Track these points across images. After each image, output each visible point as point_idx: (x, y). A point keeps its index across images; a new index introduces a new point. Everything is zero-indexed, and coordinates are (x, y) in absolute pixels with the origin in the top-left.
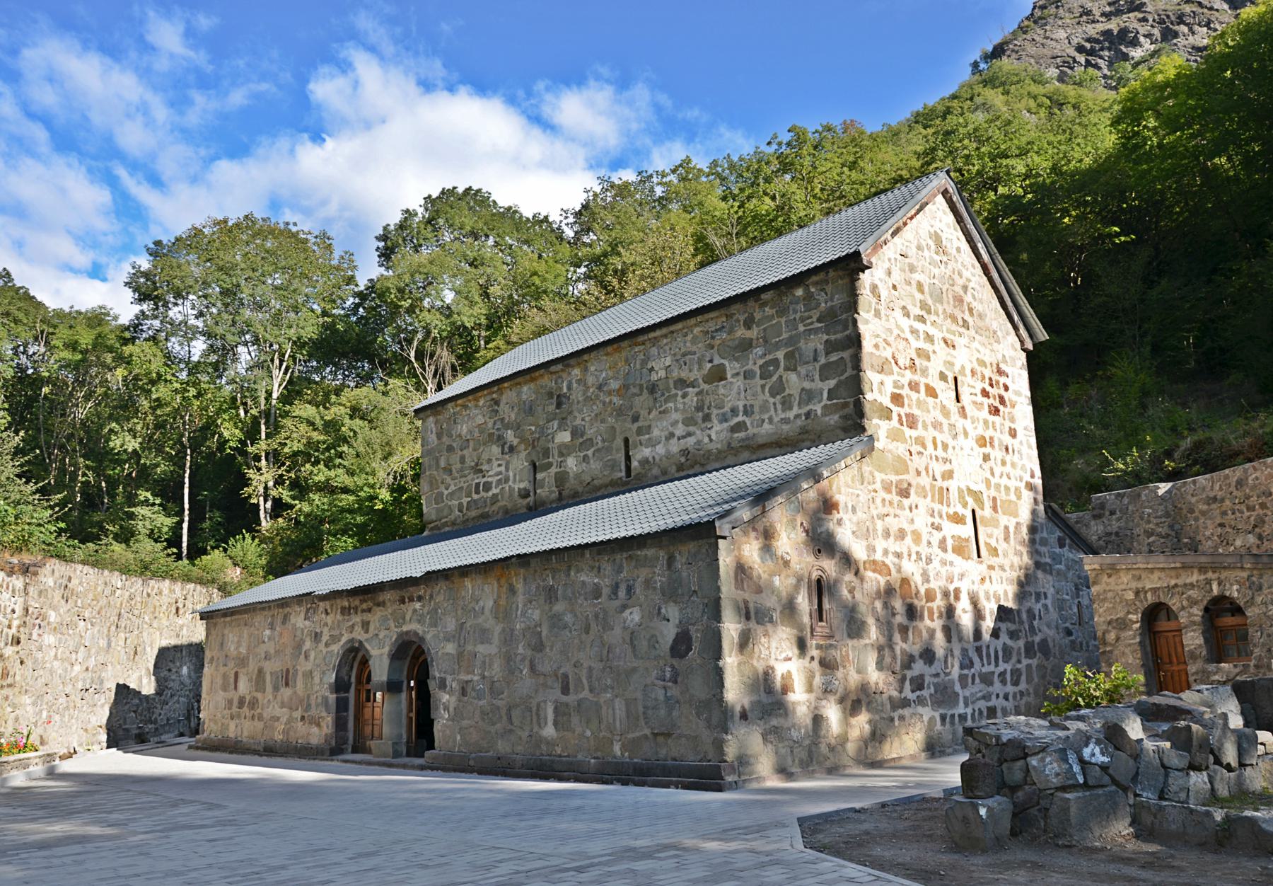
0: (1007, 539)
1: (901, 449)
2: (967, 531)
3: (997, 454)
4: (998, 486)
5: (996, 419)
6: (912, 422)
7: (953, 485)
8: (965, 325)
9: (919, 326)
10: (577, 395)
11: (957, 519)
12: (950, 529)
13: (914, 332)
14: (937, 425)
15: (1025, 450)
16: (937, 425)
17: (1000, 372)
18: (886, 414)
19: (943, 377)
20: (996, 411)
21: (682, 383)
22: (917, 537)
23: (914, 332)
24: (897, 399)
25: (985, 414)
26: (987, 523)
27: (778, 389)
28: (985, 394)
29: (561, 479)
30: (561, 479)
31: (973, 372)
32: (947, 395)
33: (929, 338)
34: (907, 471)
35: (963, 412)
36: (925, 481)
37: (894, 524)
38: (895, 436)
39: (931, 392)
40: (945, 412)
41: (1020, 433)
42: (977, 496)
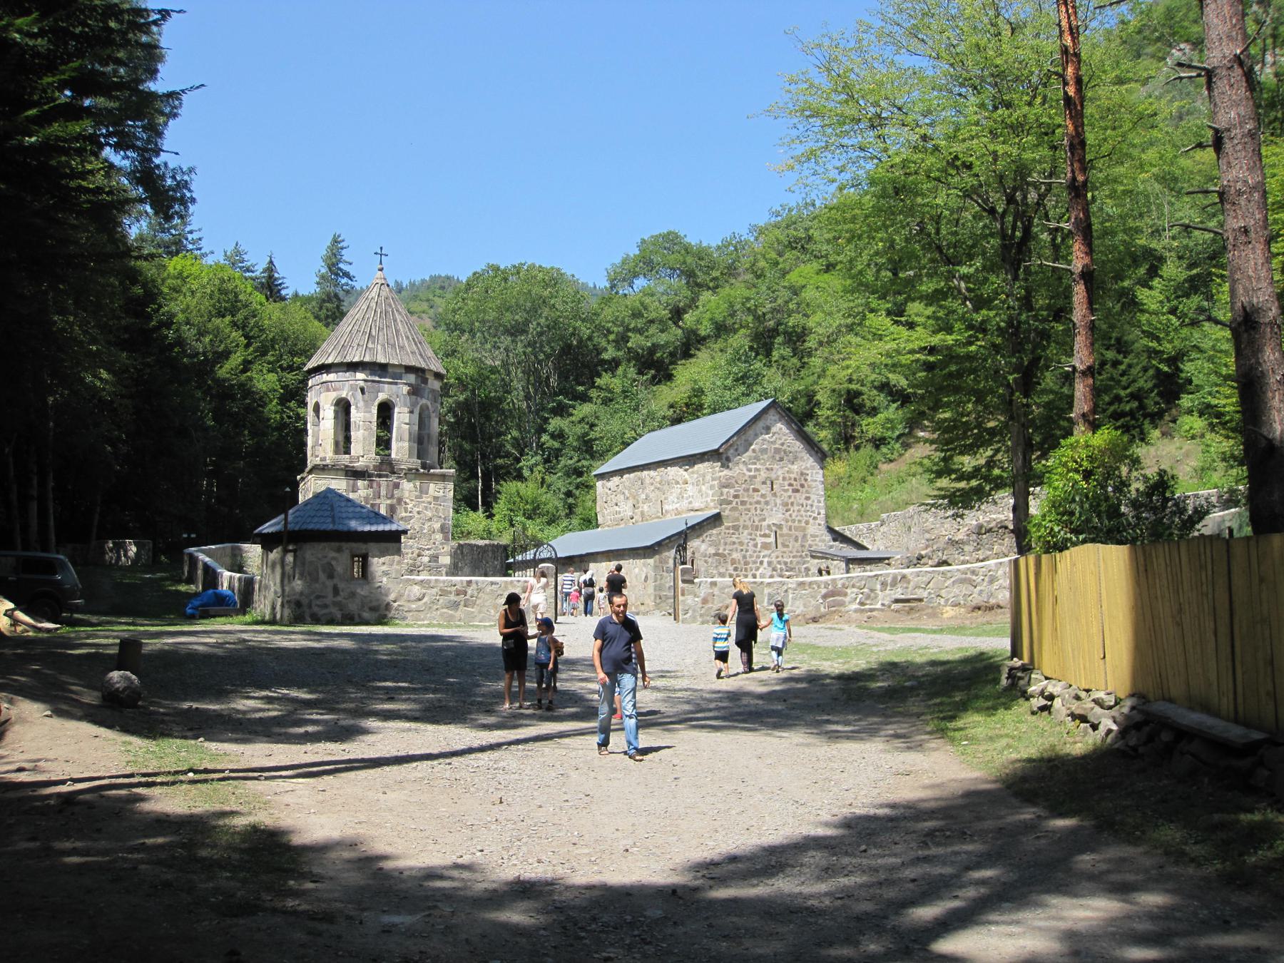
0: (796, 540)
1: (736, 514)
2: (772, 539)
3: (796, 508)
4: (794, 521)
5: (797, 495)
6: (743, 503)
7: (765, 524)
8: (781, 459)
9: (753, 467)
10: (648, 481)
11: (765, 536)
12: (760, 540)
13: (750, 470)
14: (758, 502)
15: (816, 504)
16: (758, 502)
17: (802, 474)
18: (730, 503)
19: (764, 483)
20: (797, 491)
21: (677, 483)
22: (741, 543)
23: (750, 470)
24: (736, 497)
25: (790, 493)
26: (782, 535)
27: (700, 491)
28: (790, 485)
29: (642, 513)
30: (642, 513)
31: (784, 479)
32: (765, 490)
33: (757, 470)
34: (737, 519)
35: (775, 495)
36: (749, 523)
37: (729, 540)
38: (733, 509)
39: (755, 490)
40: (763, 496)
41: (813, 497)
42: (780, 527)
